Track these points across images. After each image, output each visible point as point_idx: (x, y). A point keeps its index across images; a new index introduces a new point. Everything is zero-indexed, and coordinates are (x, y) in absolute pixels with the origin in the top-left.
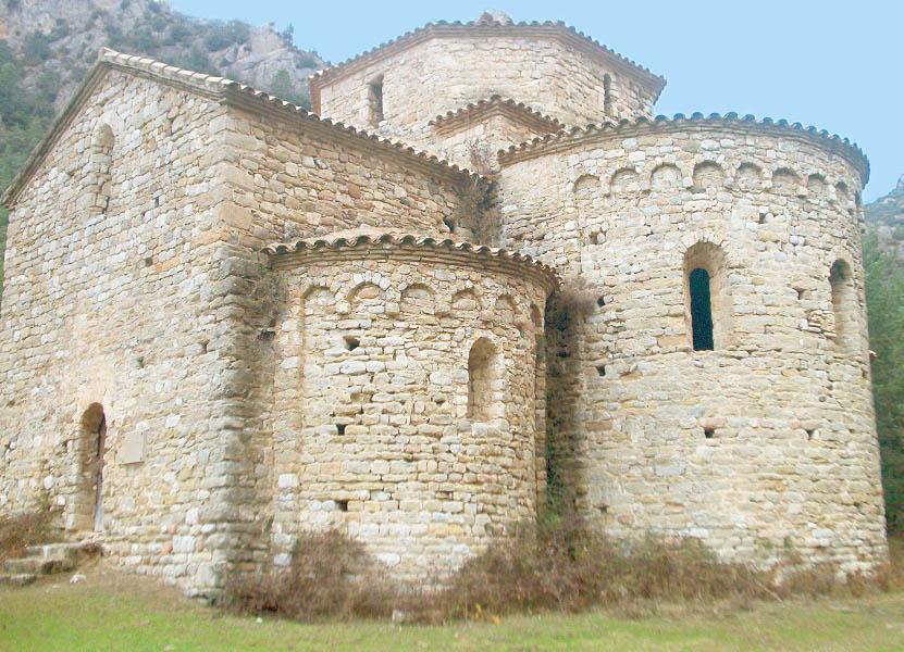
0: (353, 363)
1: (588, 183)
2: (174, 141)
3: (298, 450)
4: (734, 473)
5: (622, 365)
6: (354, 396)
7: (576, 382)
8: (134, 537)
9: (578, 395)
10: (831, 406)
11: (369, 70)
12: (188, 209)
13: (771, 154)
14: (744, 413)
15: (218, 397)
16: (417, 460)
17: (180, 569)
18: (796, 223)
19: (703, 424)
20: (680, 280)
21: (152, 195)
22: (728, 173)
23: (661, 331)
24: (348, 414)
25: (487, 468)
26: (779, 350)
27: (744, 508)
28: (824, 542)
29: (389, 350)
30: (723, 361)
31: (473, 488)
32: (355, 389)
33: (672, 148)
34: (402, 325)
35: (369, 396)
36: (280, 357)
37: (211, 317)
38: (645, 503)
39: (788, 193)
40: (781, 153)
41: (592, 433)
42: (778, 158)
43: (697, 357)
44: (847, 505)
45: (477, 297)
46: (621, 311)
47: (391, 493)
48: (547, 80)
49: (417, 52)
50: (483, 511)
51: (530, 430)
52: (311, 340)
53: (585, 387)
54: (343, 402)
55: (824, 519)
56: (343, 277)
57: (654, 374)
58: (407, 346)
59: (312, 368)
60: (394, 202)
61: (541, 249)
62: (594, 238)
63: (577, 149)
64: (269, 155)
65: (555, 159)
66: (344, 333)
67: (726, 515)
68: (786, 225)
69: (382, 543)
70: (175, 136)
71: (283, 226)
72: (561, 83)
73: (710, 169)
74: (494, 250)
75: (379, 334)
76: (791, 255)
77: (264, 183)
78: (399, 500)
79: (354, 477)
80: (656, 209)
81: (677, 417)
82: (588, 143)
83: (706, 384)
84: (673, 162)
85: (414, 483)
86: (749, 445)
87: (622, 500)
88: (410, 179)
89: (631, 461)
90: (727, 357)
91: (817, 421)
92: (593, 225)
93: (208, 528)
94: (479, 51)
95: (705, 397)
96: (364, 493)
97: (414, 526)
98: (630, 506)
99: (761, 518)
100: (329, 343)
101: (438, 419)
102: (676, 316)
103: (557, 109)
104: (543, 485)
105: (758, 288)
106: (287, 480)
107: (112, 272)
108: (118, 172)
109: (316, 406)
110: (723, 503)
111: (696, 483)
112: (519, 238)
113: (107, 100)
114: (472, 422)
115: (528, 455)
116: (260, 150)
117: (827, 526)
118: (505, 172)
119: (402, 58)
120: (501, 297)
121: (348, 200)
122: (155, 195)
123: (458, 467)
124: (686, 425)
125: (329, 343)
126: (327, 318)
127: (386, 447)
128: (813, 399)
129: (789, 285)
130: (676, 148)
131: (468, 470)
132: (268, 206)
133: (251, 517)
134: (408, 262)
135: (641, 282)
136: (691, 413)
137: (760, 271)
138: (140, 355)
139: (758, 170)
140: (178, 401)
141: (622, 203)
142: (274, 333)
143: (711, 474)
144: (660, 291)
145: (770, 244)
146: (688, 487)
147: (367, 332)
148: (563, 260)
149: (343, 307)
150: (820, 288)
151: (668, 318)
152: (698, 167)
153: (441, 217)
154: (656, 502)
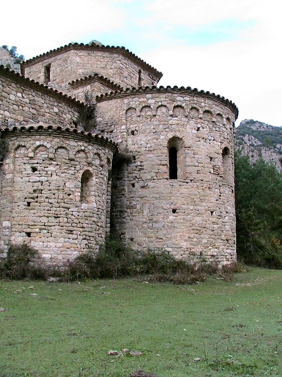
0: (34, 178)
1: (132, 110)
3: (11, 212)
4: (183, 227)
5: (141, 183)
6: (35, 191)
7: (123, 189)
9: (123, 195)
10: (220, 202)
11: (45, 61)
13: (203, 104)
14: (188, 204)
16: (59, 217)
18: (211, 132)
19: (172, 208)
20: (166, 151)
22: (186, 110)
24: (32, 198)
25: (87, 222)
26: (202, 180)
27: (186, 241)
28: (215, 254)
29: (49, 173)
30: (181, 183)
31: (81, 229)
32: (35, 188)
34: (54, 163)
35: (40, 191)
38: (148, 238)
39: (208, 120)
41: (129, 210)
42: (205, 106)
43: (170, 181)
45: (86, 153)
46: (142, 162)
47: (48, 230)
49: (65, 55)
50: (85, 239)
51: (105, 208)
52: (18, 168)
53: (127, 192)
54: (30, 193)
55: (215, 245)
56: (32, 142)
57: (153, 188)
58: (56, 171)
59: (18, 179)
61: (111, 136)
62: (133, 133)
63: (128, 97)
65: (119, 100)
66: (31, 165)
67: (179, 244)
68: (207, 132)
71: (8, 121)
72: (122, 72)
73: (180, 108)
74: (94, 135)
75: (45, 166)
76: (208, 144)
79: (34, 223)
80: (158, 123)
81: (162, 205)
83: (174, 192)
84: (165, 104)
85: (58, 226)
86: (189, 216)
87: (139, 236)
88: (60, 105)
89: (144, 221)
90: (183, 182)
91: (215, 208)
92: (133, 127)
94: (90, 56)
95: (173, 197)
96: (38, 230)
97: (57, 244)
98: (142, 238)
103: (121, 82)
104: (108, 230)
105: (196, 156)
109: (18, 195)
111: (168, 230)
112: (103, 131)
114: (82, 203)
115: (103, 217)
117: (216, 248)
120: (95, 154)
121: (34, 112)
123: (75, 221)
124: (166, 208)
126: (25, 159)
127: (47, 212)
128: (213, 200)
131: (79, 222)
135: (151, 151)
137: (196, 149)
139: (198, 110)
141: (145, 119)
142: (2, 164)
144: (158, 155)
145: (201, 139)
147: (41, 165)
148: (120, 141)
149: (31, 155)
150: (219, 157)
151: (161, 166)
152: (175, 107)
154: (152, 237)
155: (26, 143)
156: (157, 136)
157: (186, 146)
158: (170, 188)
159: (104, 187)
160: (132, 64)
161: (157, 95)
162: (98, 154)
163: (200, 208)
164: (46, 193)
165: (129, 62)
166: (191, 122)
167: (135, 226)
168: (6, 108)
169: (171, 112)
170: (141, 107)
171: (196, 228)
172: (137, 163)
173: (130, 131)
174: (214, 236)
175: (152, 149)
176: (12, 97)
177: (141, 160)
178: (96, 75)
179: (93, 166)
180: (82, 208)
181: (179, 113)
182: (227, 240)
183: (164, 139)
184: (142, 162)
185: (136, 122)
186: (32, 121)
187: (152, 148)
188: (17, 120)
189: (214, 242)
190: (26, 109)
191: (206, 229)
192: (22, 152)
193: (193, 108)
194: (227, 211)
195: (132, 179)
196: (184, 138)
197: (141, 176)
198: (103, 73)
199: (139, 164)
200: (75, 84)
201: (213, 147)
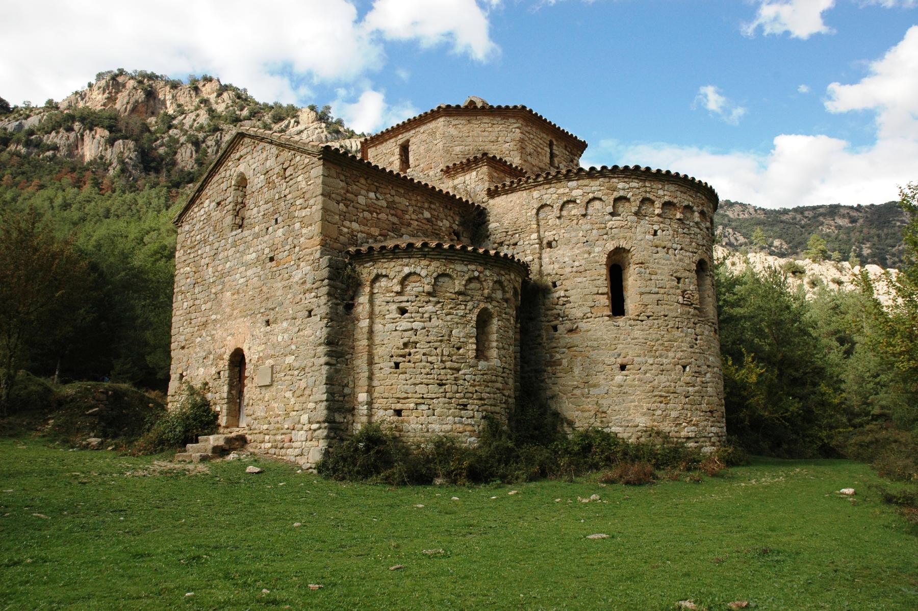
0: (404, 324)
1: (546, 209)
5: (568, 325)
6: (406, 345)
7: (539, 335)
8: (266, 432)
9: (540, 344)
11: (400, 136)
12: (297, 225)
15: (320, 345)
16: (445, 384)
17: (297, 451)
20: (604, 271)
21: (273, 217)
23: (593, 304)
24: (401, 356)
25: (488, 390)
27: (644, 414)
28: (691, 435)
29: (426, 315)
30: (632, 322)
31: (480, 402)
32: (406, 340)
37: (313, 294)
40: (664, 193)
45: (481, 282)
46: (566, 291)
49: (432, 125)
51: (512, 367)
54: (398, 348)
56: (397, 269)
62: (549, 245)
64: (348, 191)
65: (524, 193)
66: (398, 305)
70: (287, 180)
76: (673, 257)
79: (406, 395)
82: (547, 183)
86: (647, 375)
88: (433, 206)
90: (634, 320)
92: (548, 236)
93: (315, 426)
95: (621, 346)
102: (602, 294)
107: (248, 266)
108: (250, 202)
112: (501, 244)
113: (241, 156)
115: (511, 381)
116: (342, 188)
117: (694, 425)
118: (491, 202)
119: (422, 129)
120: (496, 282)
121: (395, 220)
122: (275, 217)
123: (471, 389)
128: (685, 346)
132: (347, 223)
133: (342, 420)
134: (438, 259)
138: (267, 318)
140: (293, 347)
141: (567, 222)
144: (593, 278)
152: (617, 200)
153: (451, 230)
159: (511, 333)
160: (538, 132)
161: (586, 182)
162: (499, 282)
164: (422, 347)
165: (534, 129)
168: (354, 218)
170: (561, 202)
173: (545, 242)
175: (581, 269)
176: (361, 200)
177: (565, 288)
178: (485, 154)
180: (480, 368)
182: (711, 412)
183: (601, 252)
184: (566, 291)
188: (370, 235)
190: (383, 216)
191: (676, 395)
195: (552, 318)
198: (494, 150)
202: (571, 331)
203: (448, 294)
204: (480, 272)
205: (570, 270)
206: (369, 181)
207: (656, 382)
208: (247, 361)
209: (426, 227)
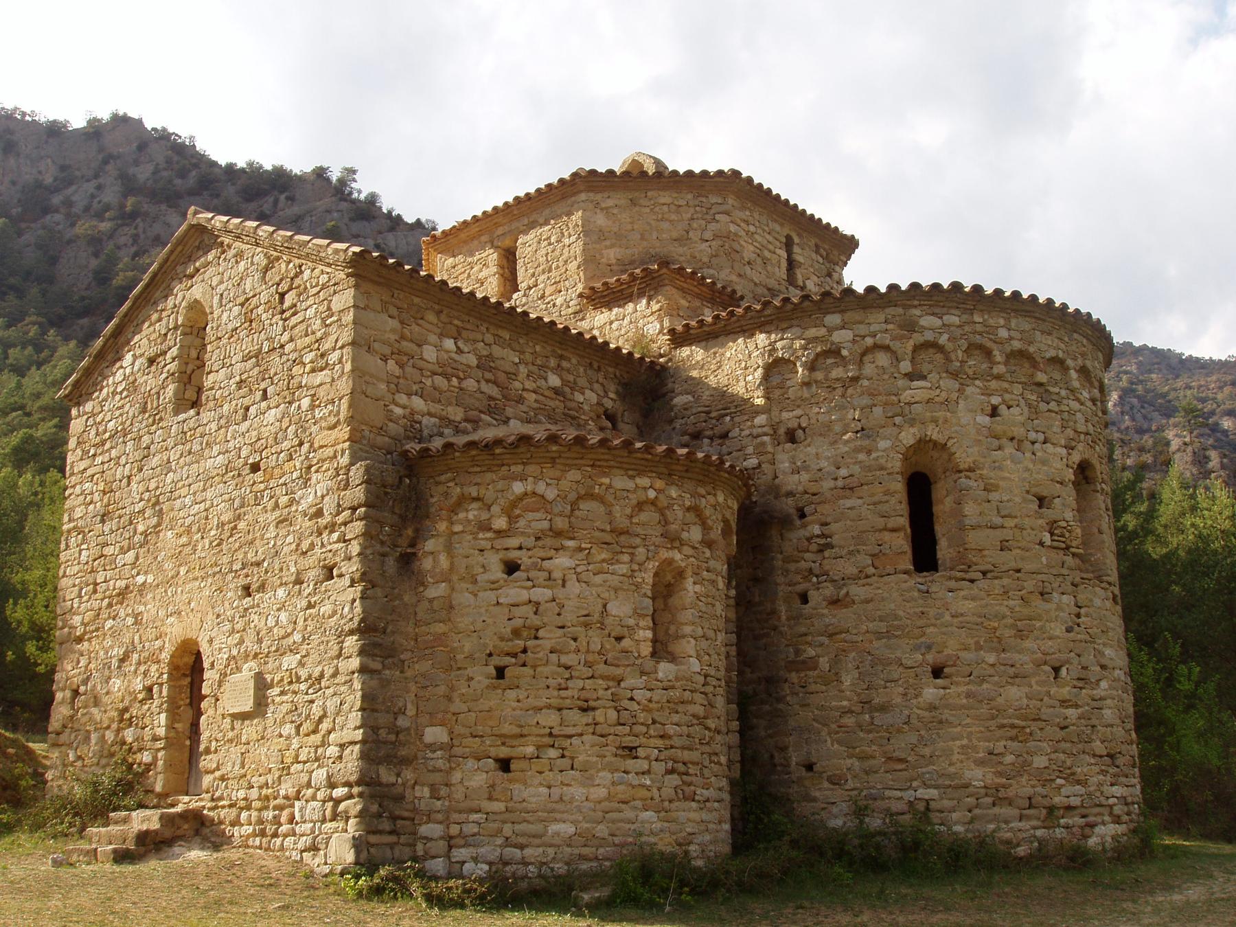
0: (514, 592)
2: (285, 320)
3: (450, 699)
4: (968, 720)
5: (829, 590)
6: (516, 633)
7: (774, 612)
9: (775, 628)
13: (1003, 333)
14: (979, 648)
15: (351, 632)
16: (594, 709)
17: (304, 842)
20: (899, 486)
22: (953, 356)
26: (1019, 571)
27: (980, 763)
28: (1075, 801)
30: (952, 584)
32: (518, 623)
33: (884, 326)
34: (571, 543)
35: (533, 632)
36: (423, 584)
38: (860, 758)
41: (793, 674)
43: (920, 580)
44: (1101, 756)
46: (827, 524)
47: (563, 749)
48: (720, 243)
51: (722, 673)
52: (461, 564)
53: (784, 618)
54: (502, 639)
57: (867, 601)
59: (463, 598)
60: (547, 393)
61: (725, 449)
62: (791, 437)
64: (403, 337)
66: (501, 555)
69: (553, 811)
70: (287, 314)
71: (420, 423)
72: (737, 247)
73: (931, 350)
76: (1028, 455)
77: (398, 371)
78: (572, 758)
79: (518, 731)
80: (866, 401)
81: (899, 654)
82: (781, 320)
83: (932, 612)
84: (887, 342)
85: (591, 736)
86: (985, 686)
87: (832, 754)
88: (565, 364)
89: (844, 707)
90: (957, 579)
91: (1064, 656)
94: (637, 208)
95: (931, 629)
96: (530, 750)
97: (592, 790)
99: (1000, 774)
100: (483, 566)
101: (618, 659)
102: (894, 530)
103: (734, 278)
104: (734, 739)
105: (994, 496)
106: (435, 734)
108: (213, 356)
110: (955, 757)
111: (923, 732)
112: (697, 436)
114: (658, 662)
115: (720, 702)
116: (393, 331)
117: (1078, 782)
120: (688, 509)
121: (493, 391)
122: (263, 385)
124: (909, 663)
125: (483, 566)
128: (1058, 630)
129: (1028, 492)
130: (890, 327)
131: (654, 722)
132: (402, 398)
133: (392, 779)
135: (851, 489)
136: (916, 648)
137: (992, 474)
139: (988, 353)
141: (823, 393)
142: (414, 554)
143: (941, 722)
144: (876, 499)
145: (1004, 441)
146: (914, 740)
148: (753, 462)
149: (501, 523)
150: (1064, 494)
151: (886, 533)
152: (917, 349)
153: (601, 410)
154: (874, 758)
155: (483, 492)
156: (867, 442)
157: (961, 467)
158: (921, 602)
159: (719, 608)
160: (764, 219)
162: (695, 510)
163: (1017, 657)
164: (550, 637)
166: (969, 390)
167: (816, 725)
168: (415, 387)
169: (906, 366)
171: (1010, 721)
172: (809, 528)
173: (782, 431)
174: (1069, 745)
175: (853, 482)
176: (430, 353)
177: (823, 519)
179: (685, 548)
181: (931, 366)
183: (890, 450)
184: (827, 524)
185: (799, 402)
186: (488, 418)
187: (855, 479)
188: (446, 421)
189: (1068, 763)
190: (470, 384)
192: (471, 516)
193: (972, 348)
194: (1103, 661)
195: (799, 578)
196: (952, 441)
197: (827, 568)
199: (816, 530)
200: (603, 297)
201: (1044, 462)
202: (835, 602)
203: (597, 534)
204: (659, 491)
205: (832, 484)
206: (443, 317)
207: (1000, 700)
208: (206, 665)
209: (552, 404)
